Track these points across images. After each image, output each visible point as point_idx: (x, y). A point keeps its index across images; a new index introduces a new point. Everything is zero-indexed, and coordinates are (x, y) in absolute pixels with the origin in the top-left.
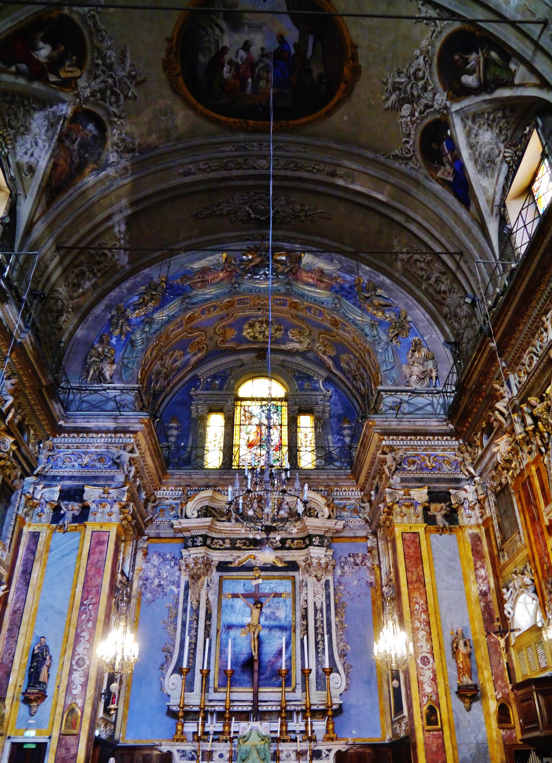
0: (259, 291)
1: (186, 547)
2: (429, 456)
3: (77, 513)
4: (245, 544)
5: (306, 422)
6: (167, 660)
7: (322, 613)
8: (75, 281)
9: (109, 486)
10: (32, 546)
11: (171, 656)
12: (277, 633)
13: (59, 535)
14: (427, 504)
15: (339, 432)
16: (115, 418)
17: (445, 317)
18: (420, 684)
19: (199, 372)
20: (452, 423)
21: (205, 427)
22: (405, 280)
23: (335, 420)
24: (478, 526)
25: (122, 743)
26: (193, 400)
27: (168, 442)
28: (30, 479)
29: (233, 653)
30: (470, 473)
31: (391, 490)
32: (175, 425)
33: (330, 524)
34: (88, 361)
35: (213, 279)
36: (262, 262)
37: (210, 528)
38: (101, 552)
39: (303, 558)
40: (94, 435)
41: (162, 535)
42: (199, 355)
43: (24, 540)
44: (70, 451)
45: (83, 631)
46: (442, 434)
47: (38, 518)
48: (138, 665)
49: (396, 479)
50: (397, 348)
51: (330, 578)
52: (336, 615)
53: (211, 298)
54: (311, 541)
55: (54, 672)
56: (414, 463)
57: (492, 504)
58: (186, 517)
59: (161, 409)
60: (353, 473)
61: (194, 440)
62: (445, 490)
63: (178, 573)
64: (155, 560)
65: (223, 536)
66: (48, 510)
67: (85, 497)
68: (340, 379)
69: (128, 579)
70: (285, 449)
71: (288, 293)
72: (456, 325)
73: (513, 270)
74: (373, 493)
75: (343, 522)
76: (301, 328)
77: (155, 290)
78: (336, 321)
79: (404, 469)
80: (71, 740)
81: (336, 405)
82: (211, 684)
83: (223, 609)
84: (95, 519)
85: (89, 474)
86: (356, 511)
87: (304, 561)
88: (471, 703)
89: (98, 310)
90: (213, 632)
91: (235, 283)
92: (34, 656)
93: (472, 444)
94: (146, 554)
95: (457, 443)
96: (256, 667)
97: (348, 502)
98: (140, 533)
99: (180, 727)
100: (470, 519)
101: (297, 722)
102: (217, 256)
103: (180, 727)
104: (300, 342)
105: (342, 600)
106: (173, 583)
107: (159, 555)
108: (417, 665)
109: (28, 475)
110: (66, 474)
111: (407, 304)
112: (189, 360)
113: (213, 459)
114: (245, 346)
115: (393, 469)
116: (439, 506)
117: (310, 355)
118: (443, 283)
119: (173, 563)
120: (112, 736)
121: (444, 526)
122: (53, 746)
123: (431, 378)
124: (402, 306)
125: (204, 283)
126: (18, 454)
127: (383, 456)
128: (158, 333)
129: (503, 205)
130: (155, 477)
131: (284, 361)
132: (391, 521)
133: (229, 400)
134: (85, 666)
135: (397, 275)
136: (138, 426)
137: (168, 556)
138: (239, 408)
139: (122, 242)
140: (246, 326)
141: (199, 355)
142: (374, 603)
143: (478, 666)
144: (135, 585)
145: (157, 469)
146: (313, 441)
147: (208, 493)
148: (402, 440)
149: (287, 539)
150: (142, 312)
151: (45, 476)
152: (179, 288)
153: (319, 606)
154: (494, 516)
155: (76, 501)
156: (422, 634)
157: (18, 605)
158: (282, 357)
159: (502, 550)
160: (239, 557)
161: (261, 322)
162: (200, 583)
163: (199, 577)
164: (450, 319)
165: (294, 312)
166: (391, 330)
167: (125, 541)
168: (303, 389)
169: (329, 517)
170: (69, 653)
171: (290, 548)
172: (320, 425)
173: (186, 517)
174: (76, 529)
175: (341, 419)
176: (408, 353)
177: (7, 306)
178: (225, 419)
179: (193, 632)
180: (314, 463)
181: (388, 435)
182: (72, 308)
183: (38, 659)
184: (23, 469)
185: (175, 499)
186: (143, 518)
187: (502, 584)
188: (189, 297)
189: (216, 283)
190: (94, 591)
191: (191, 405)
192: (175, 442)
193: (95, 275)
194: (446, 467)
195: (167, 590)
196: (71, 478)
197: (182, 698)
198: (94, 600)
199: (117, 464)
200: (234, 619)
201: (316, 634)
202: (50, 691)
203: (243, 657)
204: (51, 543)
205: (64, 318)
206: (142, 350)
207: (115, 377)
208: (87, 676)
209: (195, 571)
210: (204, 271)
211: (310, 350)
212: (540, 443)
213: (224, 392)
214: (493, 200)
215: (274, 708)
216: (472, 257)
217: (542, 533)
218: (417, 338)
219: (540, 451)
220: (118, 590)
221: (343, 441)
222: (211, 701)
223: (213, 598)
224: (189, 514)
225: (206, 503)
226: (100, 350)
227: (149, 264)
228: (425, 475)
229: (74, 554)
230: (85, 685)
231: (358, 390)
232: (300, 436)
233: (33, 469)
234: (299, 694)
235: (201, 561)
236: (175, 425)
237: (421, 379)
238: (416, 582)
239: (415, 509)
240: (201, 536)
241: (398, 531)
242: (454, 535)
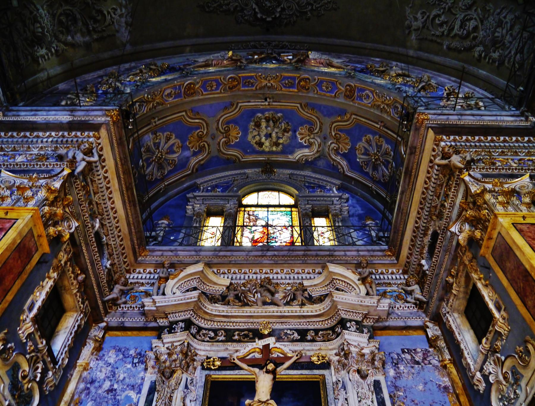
4: (246, 336)
22: (421, 54)
23: (357, 218)
26: (190, 202)
37: (197, 308)
39: (335, 352)
41: (127, 325)
42: (200, 157)
51: (381, 378)
59: (153, 206)
64: (112, 357)
65: (215, 326)
74: (423, 262)
76: (311, 123)
81: (354, 207)
87: (336, 355)
94: (99, 349)
97: (389, 289)
106: (133, 387)
107: (120, 350)
112: (188, 159)
130: (129, 251)
131: (292, 174)
135: (411, 53)
138: (242, 213)
139: (124, 10)
141: (200, 157)
149: (308, 330)
158: (289, 171)
160: (237, 351)
161: (268, 120)
162: (173, 381)
163: (173, 372)
165: (303, 94)
169: (368, 294)
171: (313, 341)
173: (164, 294)
195: (121, 397)
205: (43, 52)
209: (168, 364)
211: (321, 156)
235: (179, 349)
240: (182, 321)
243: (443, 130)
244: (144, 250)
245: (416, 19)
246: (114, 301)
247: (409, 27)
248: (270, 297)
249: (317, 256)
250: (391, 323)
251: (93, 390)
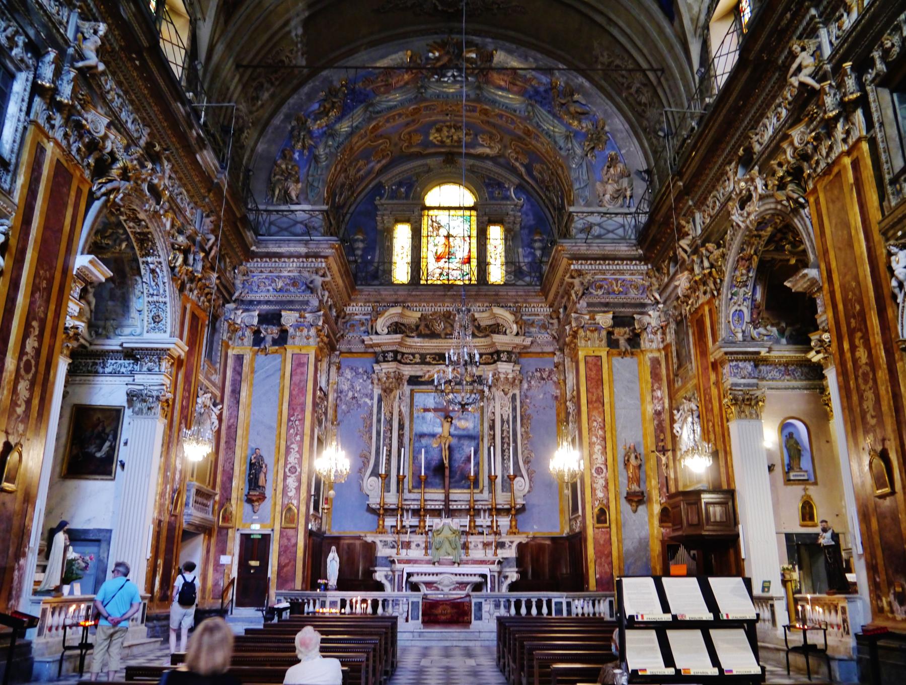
0: (448, 97)
1: (377, 362)
2: (617, 280)
3: (276, 337)
4: (434, 359)
5: (496, 233)
6: (365, 464)
7: (508, 423)
8: (254, 94)
9: (305, 310)
10: (237, 368)
11: (368, 462)
12: (466, 442)
13: (261, 357)
14: (611, 329)
15: (530, 245)
16: (306, 243)
17: (644, 130)
18: (593, 490)
19: (383, 179)
20: (641, 248)
21: (391, 239)
23: (526, 231)
24: (659, 350)
25: (328, 534)
26: (379, 210)
27: (355, 255)
28: (231, 306)
29: (426, 458)
30: (655, 299)
31: (576, 315)
32: (360, 237)
33: (518, 340)
34: (273, 180)
35: (398, 82)
36: (450, 60)
37: (400, 344)
38: (302, 374)
40: (286, 260)
41: (353, 350)
42: (384, 162)
43: (230, 362)
44: (264, 275)
45: (292, 443)
46: (631, 259)
47: (240, 342)
48: (348, 475)
49: (583, 303)
50: (591, 163)
51: (517, 392)
52: (522, 426)
53: (395, 106)
54: (499, 356)
55: (270, 476)
56: (601, 287)
57: (673, 331)
58: (377, 333)
60: (542, 290)
61: (381, 254)
62: (630, 314)
63: (370, 386)
64: (348, 374)
65: (413, 351)
66: (248, 333)
67: (283, 321)
68: (532, 187)
69: (325, 395)
70: (474, 262)
71: (478, 100)
72: (654, 140)
73: (708, 105)
75: (530, 339)
77: (336, 96)
78: (529, 130)
79: (591, 293)
80: (291, 532)
81: (527, 215)
82: (406, 486)
83: (415, 420)
84: (294, 343)
85: (284, 299)
86: (544, 327)
88: (637, 506)
89: (277, 121)
90: (406, 440)
91: (422, 87)
92: (251, 465)
93: (659, 270)
94: (339, 368)
95: (646, 267)
96: (447, 472)
98: (332, 349)
99: (381, 522)
100: (651, 344)
101: (484, 518)
102: (401, 54)
103: (381, 522)
104: (490, 147)
105: (529, 412)
106: (367, 396)
107: (352, 369)
108: (592, 474)
109: (228, 302)
110: (262, 299)
111: (605, 112)
113: (401, 274)
114: (432, 150)
115: (580, 294)
116: (622, 330)
117: (502, 160)
118: (643, 94)
119: (365, 377)
120: (320, 529)
121: (626, 350)
123: (625, 197)
124: (600, 115)
125: (389, 88)
126: (221, 288)
127: (570, 280)
128: (342, 147)
129: (706, 27)
131: (472, 166)
132: (576, 345)
133: (416, 210)
135: (596, 78)
136: (329, 251)
137: (360, 370)
138: (426, 218)
139: (299, 46)
140: (433, 131)
141: (384, 162)
142: (558, 415)
143: (647, 476)
144: (331, 397)
145: (346, 288)
146: (503, 254)
147: (398, 310)
148: (591, 264)
150: (324, 122)
151: (242, 301)
152: (361, 93)
153: (505, 418)
154: (673, 343)
155: (274, 325)
156: (598, 448)
157: (232, 421)
159: (677, 375)
160: (428, 371)
161: (449, 127)
162: (392, 396)
163: (391, 391)
164: (649, 133)
165: (484, 118)
166: (587, 143)
167: (321, 361)
168: (492, 198)
169: (517, 334)
170: (282, 462)
172: (510, 237)
173: (377, 333)
174: (276, 352)
175: (532, 230)
176: (602, 169)
177: (205, 152)
178: (412, 230)
179: (387, 441)
180: (503, 280)
181: (577, 259)
182: (252, 123)
183: (255, 469)
184: (224, 297)
185: (365, 314)
186: (335, 335)
187: (674, 406)
188: (372, 105)
189: (401, 87)
190: (299, 409)
191: (376, 215)
192: (362, 256)
193: (272, 84)
194: (633, 293)
196: (267, 302)
197: (382, 498)
198: (300, 417)
199: (310, 288)
200: (425, 429)
201: (503, 443)
202: (268, 493)
203: (434, 463)
204: (255, 365)
205: (245, 134)
206: (327, 166)
207: (302, 197)
208: (299, 481)
210: (389, 71)
211: (500, 155)
212: (713, 287)
213: (410, 202)
214: (698, 19)
215: (463, 507)
216: (672, 75)
217: (708, 368)
218: (613, 153)
219: (713, 295)
220: (318, 404)
221: (534, 255)
222: (406, 500)
223: (405, 410)
224: (379, 330)
225: (396, 319)
226: (284, 166)
227: (329, 65)
228: (611, 299)
229: (278, 374)
230: (298, 489)
231: (551, 200)
232: (490, 248)
233: (231, 295)
234: (486, 495)
235: (392, 375)
236: (360, 237)
237: (614, 198)
238: (596, 402)
239: (599, 334)
240: (391, 351)
241: (581, 354)
242: (635, 358)
243: (576, 257)
244: (355, 290)
245: (603, 56)
246: (342, 336)
247: (597, 58)
248: (450, 328)
249: (486, 295)
250: (532, 350)
251: (343, 398)
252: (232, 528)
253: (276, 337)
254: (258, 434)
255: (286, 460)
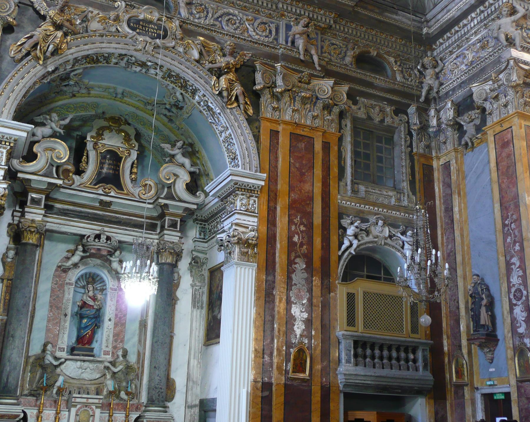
13: (470, 157)
40: (465, 22)
44: (454, 56)
45: (512, 257)
122: (514, 397)
134: (524, 298)
157: (450, 247)
190: (512, 206)
198: (515, 217)
252: (467, 385)
253: (478, 122)
254: (479, 256)
255: (509, 282)
